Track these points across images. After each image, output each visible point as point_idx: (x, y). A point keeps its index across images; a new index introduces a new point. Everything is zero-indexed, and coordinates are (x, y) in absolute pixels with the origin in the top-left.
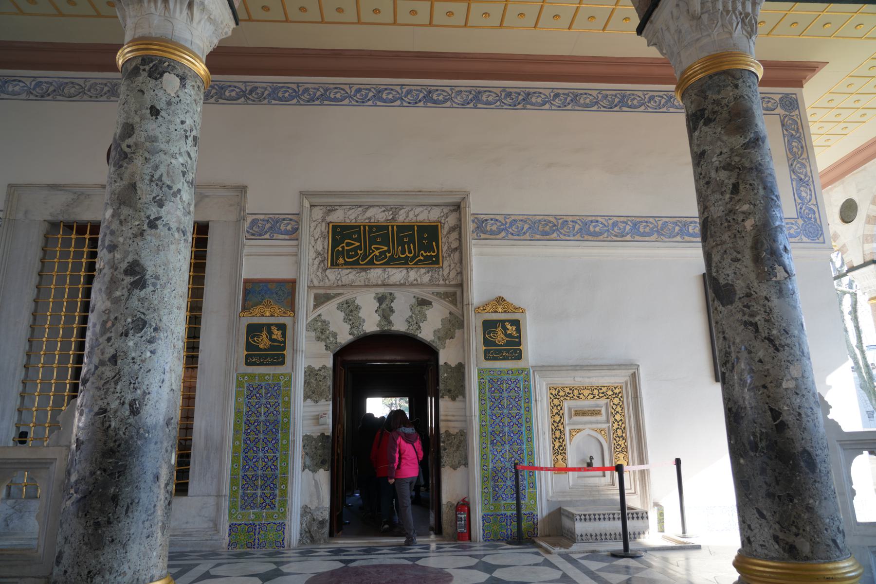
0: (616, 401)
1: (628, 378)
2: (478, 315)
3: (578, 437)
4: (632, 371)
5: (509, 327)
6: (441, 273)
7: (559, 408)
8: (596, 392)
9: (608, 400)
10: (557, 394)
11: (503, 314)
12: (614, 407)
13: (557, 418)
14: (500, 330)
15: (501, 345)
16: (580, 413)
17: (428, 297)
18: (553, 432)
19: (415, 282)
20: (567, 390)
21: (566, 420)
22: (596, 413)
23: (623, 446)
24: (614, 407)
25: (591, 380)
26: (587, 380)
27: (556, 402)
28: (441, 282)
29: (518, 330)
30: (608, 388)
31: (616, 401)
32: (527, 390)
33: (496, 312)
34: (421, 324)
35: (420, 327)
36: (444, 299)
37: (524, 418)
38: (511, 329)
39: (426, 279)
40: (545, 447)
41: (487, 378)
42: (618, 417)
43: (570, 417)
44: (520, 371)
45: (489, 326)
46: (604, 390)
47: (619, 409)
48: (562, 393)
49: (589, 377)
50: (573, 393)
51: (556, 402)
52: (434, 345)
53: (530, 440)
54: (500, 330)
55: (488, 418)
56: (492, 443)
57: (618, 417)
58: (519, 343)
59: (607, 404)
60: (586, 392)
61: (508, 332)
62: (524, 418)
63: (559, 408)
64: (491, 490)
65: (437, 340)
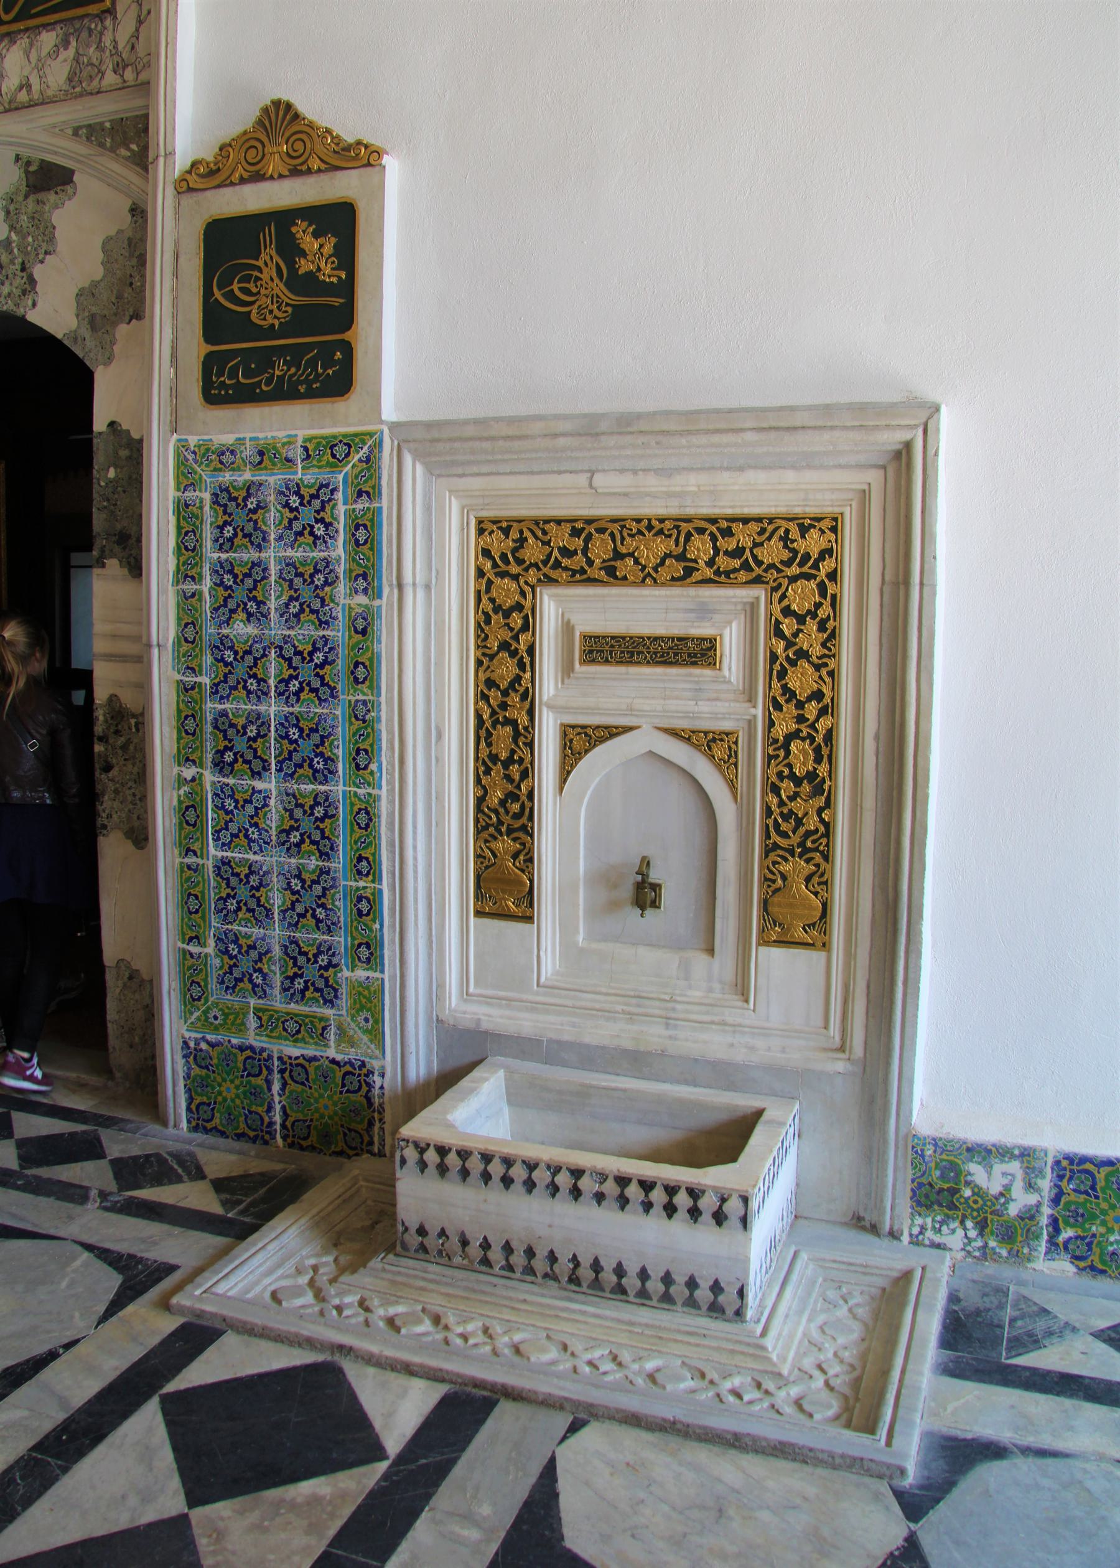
0: (802, 596)
1: (873, 477)
2: (188, 200)
3: (599, 762)
4: (893, 439)
5: (308, 242)
6: (107, 40)
7: (517, 620)
8: (701, 548)
9: (759, 593)
10: (520, 558)
11: (288, 184)
12: (788, 626)
13: (506, 668)
14: (269, 258)
15: (270, 332)
16: (604, 650)
17: (63, 150)
18: (483, 732)
19: (23, 96)
20: (561, 538)
21: (548, 682)
22: (697, 652)
23: (812, 822)
24: (788, 626)
25: (678, 483)
26: (652, 483)
27: (506, 591)
28: (110, 78)
29: (346, 255)
30: (766, 525)
31: (802, 596)
32: (365, 534)
33: (258, 177)
34: (38, 271)
35: (32, 281)
36: (112, 150)
37: (341, 664)
38: (316, 251)
39: (58, 74)
40: (434, 798)
41: (210, 479)
42: (802, 679)
43: (567, 669)
44: (336, 449)
45: (229, 245)
46: (744, 537)
47: (811, 639)
48: (533, 552)
49: (665, 472)
50: (594, 550)
51: (506, 591)
52: (78, 351)
53: (362, 758)
54: (269, 258)
55: (208, 659)
56: (219, 765)
57: (802, 679)
58: (345, 317)
59: (753, 606)
60: (652, 549)
61: (304, 266)
62: (341, 664)
63: (517, 620)
64: (210, 948)
65: (86, 332)
